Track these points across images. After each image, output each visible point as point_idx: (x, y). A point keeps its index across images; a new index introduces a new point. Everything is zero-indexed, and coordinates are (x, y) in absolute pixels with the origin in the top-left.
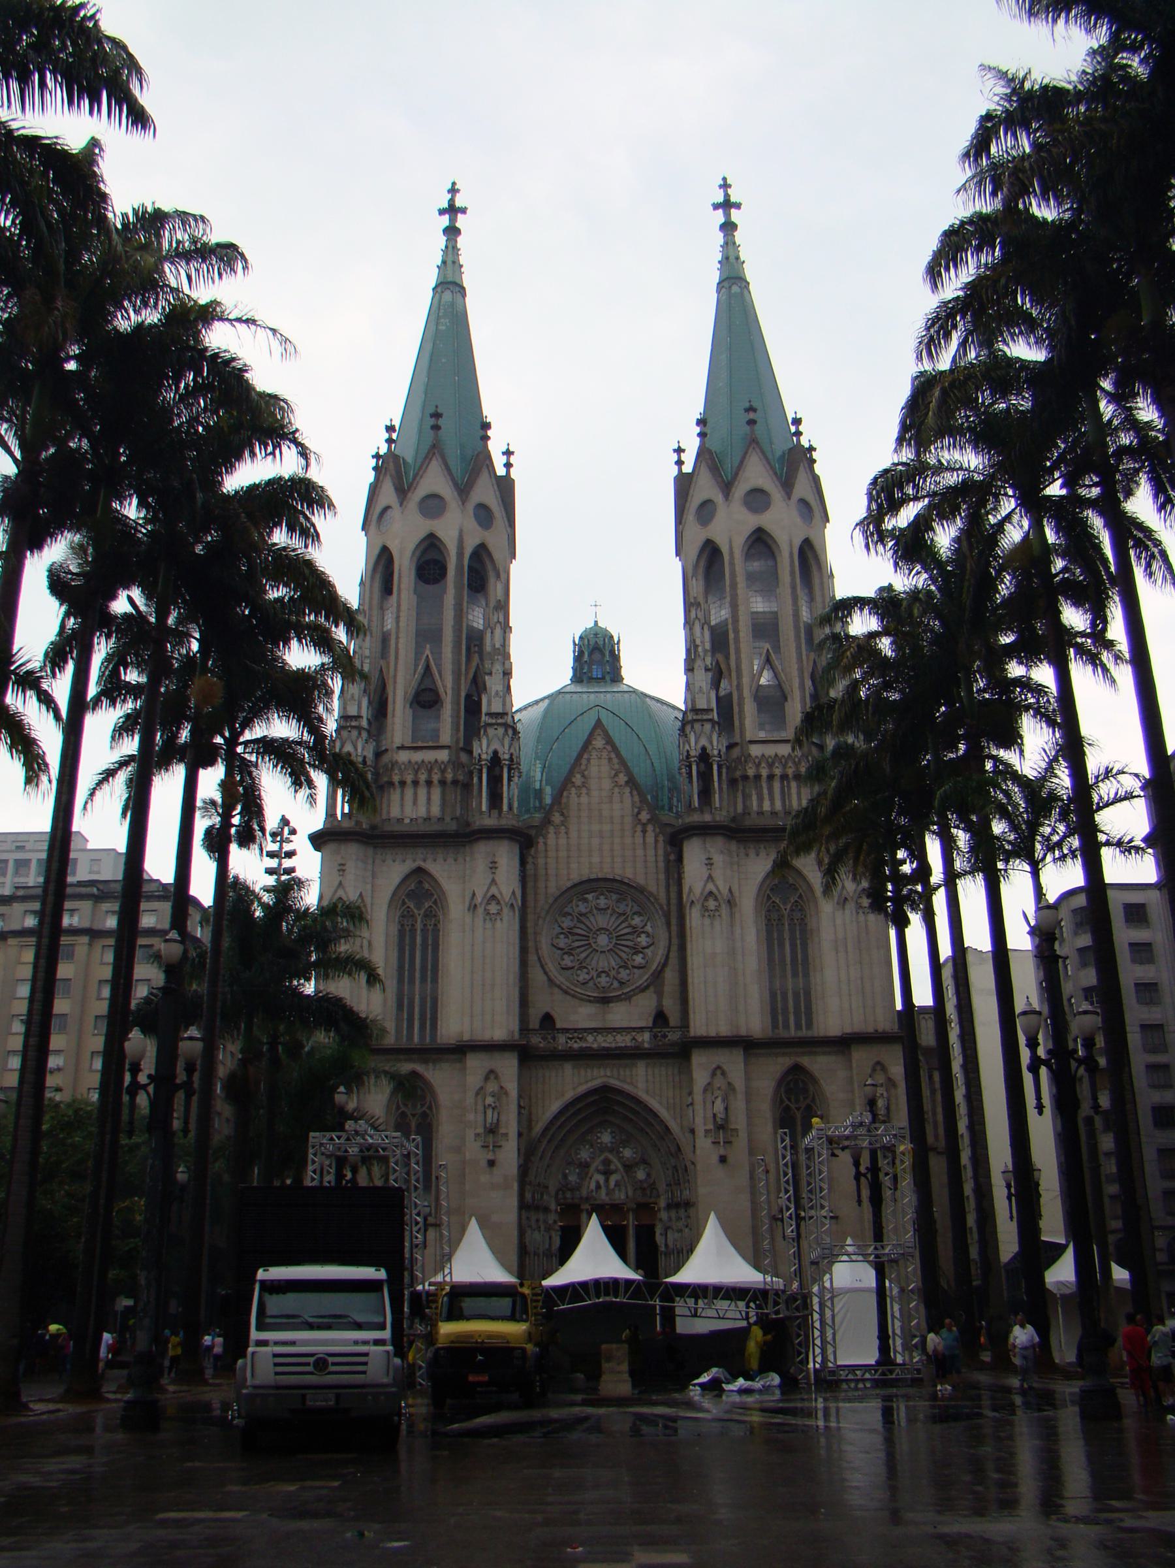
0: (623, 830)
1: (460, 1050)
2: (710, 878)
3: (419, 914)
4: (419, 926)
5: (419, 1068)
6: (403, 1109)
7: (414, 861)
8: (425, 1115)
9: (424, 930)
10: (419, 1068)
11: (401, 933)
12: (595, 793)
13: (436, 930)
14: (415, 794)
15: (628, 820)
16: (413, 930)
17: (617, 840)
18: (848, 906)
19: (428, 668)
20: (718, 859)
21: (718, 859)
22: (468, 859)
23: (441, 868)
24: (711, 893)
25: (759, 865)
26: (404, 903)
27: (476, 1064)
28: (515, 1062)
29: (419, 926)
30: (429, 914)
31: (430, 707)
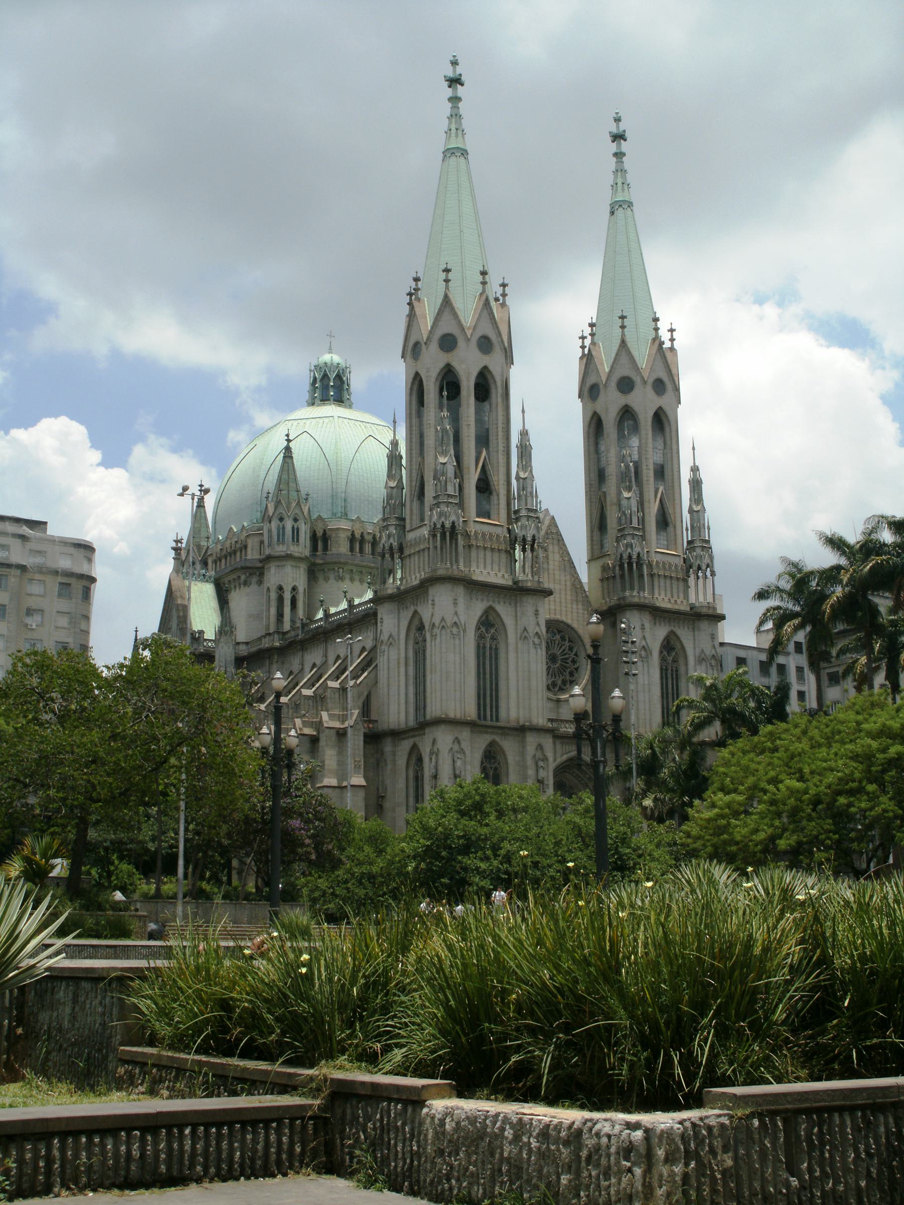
0: (566, 590)
1: (521, 730)
2: (644, 637)
3: (488, 636)
4: (488, 646)
5: (497, 738)
6: (485, 764)
7: (488, 601)
8: (496, 769)
9: (491, 648)
10: (497, 738)
11: (478, 647)
12: (551, 563)
13: (496, 649)
14: (485, 555)
15: (569, 583)
16: (484, 648)
17: (563, 596)
18: (704, 663)
19: (483, 466)
20: (647, 625)
21: (647, 625)
22: (518, 605)
23: (504, 610)
24: (643, 647)
25: (661, 632)
26: (479, 629)
27: (531, 740)
28: (551, 740)
29: (488, 646)
30: (493, 638)
31: (484, 492)
